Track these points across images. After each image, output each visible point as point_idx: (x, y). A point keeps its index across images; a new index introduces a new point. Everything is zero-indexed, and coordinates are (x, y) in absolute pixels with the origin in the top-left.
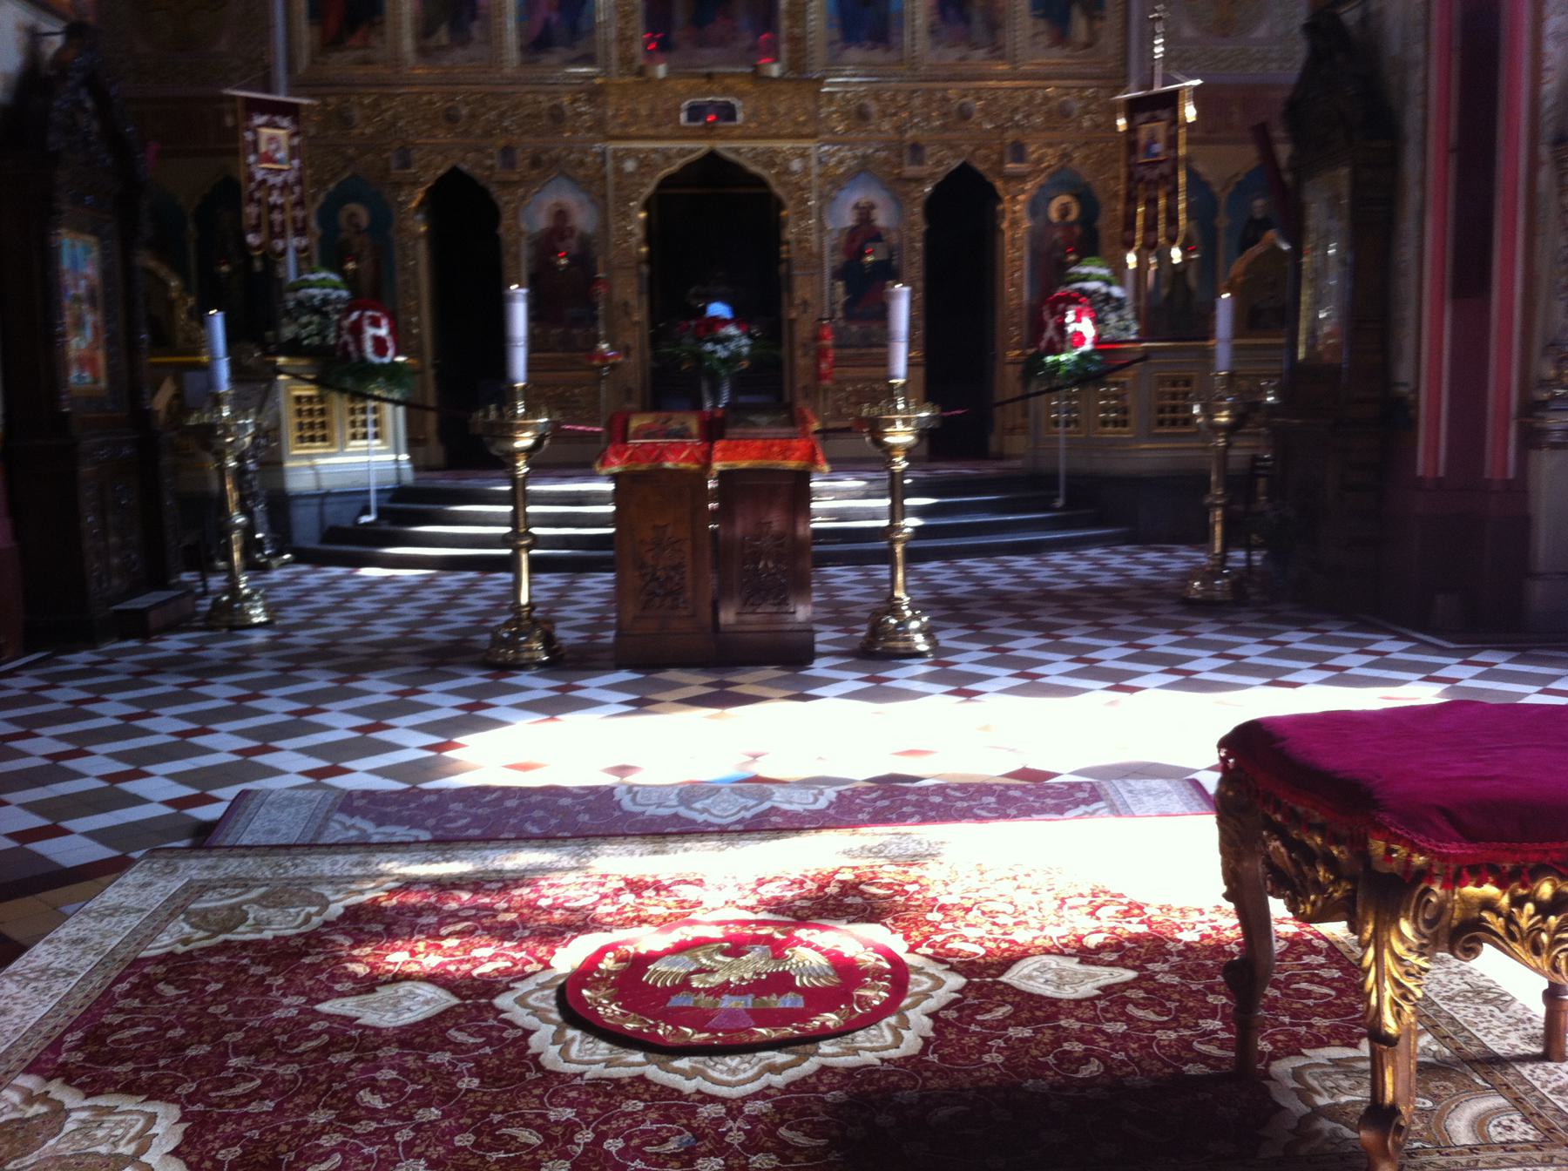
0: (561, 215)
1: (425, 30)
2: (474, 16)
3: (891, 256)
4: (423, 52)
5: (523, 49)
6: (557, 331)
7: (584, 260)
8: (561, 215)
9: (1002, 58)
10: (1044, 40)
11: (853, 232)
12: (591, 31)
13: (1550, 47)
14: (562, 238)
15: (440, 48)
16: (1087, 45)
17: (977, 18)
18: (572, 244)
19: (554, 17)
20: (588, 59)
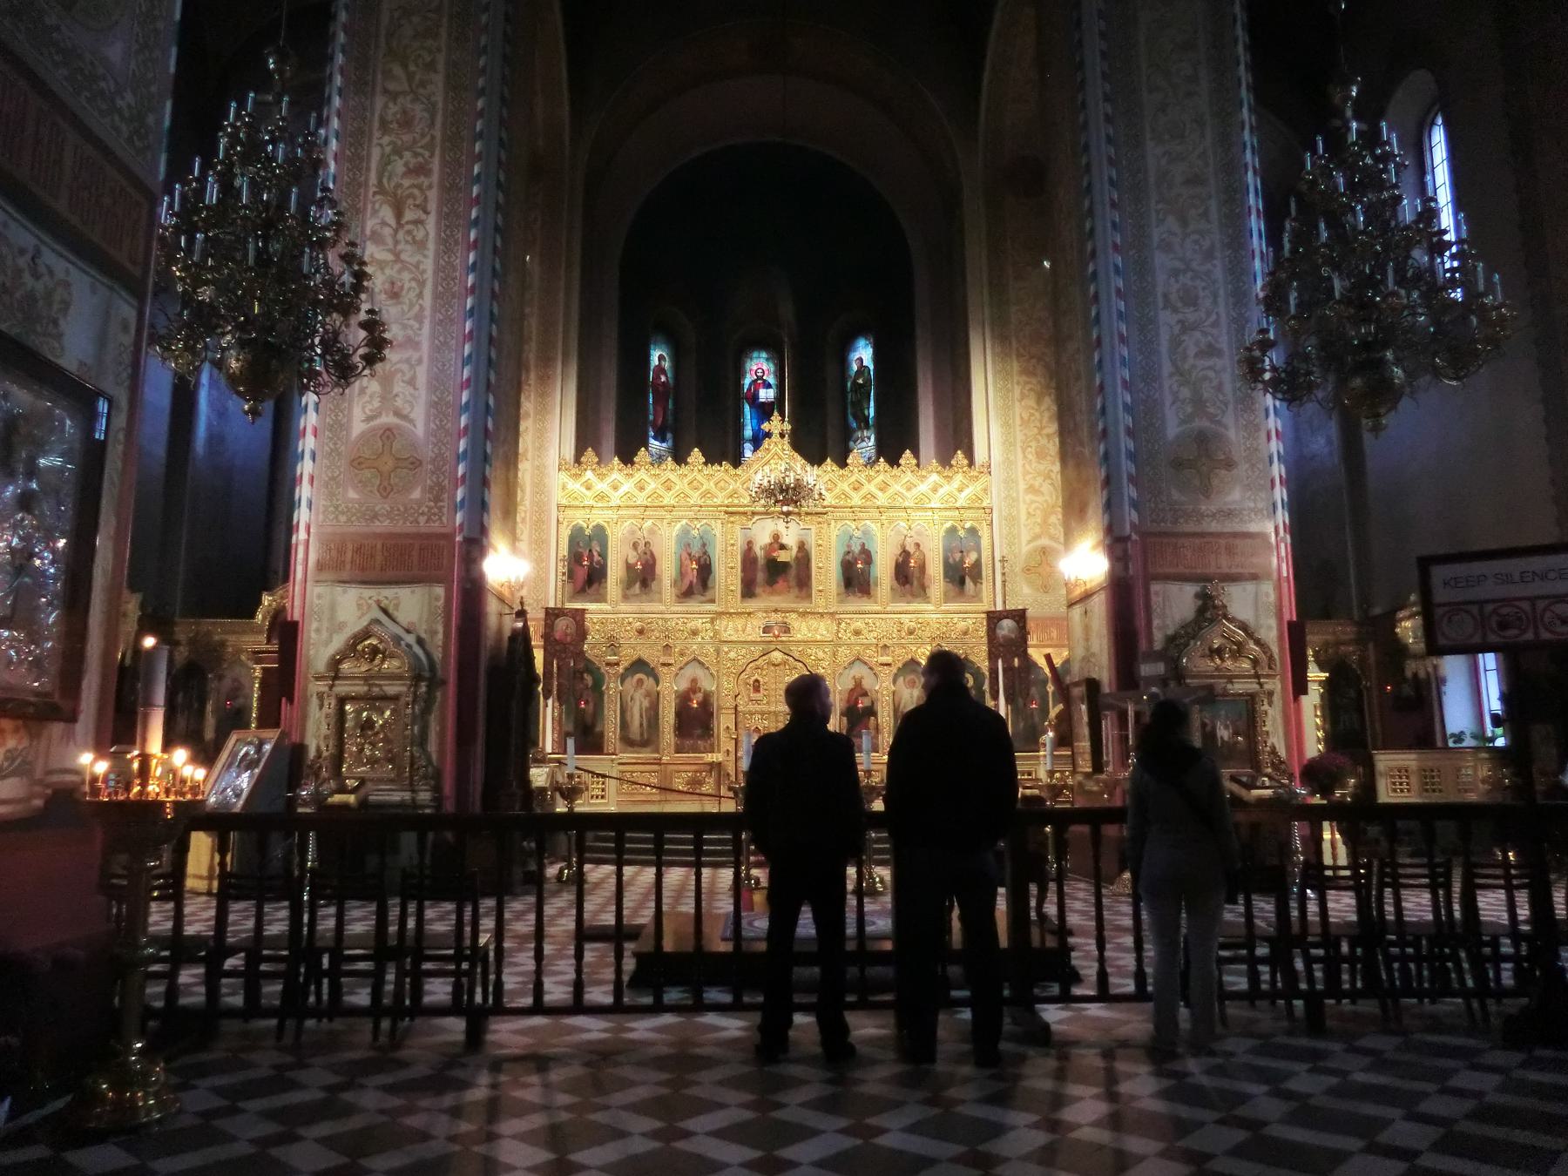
0: (694, 681)
1: (629, 584)
2: (653, 579)
3: (873, 703)
4: (626, 598)
5: (678, 596)
6: (688, 742)
7: (706, 704)
8: (694, 681)
9: (929, 602)
10: (952, 594)
11: (852, 690)
12: (714, 587)
13: (1155, 631)
14: (695, 692)
15: (637, 595)
16: (973, 597)
17: (915, 583)
18: (700, 696)
19: (695, 581)
20: (713, 601)
